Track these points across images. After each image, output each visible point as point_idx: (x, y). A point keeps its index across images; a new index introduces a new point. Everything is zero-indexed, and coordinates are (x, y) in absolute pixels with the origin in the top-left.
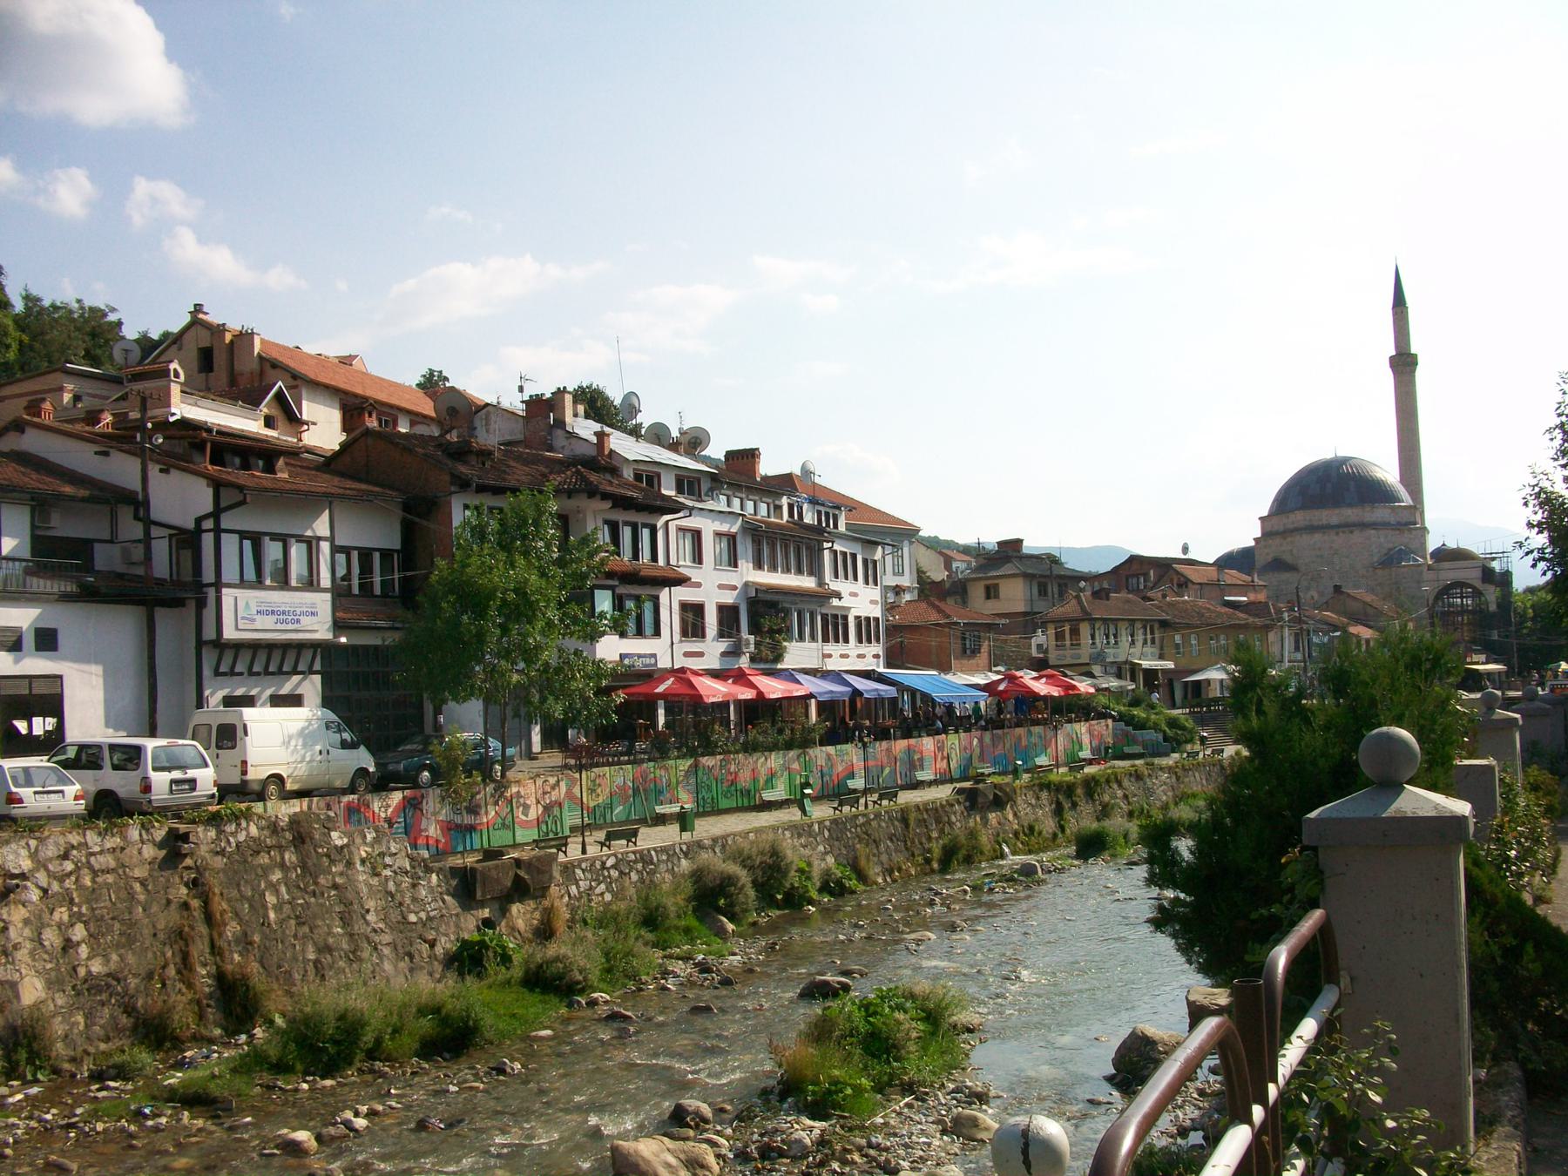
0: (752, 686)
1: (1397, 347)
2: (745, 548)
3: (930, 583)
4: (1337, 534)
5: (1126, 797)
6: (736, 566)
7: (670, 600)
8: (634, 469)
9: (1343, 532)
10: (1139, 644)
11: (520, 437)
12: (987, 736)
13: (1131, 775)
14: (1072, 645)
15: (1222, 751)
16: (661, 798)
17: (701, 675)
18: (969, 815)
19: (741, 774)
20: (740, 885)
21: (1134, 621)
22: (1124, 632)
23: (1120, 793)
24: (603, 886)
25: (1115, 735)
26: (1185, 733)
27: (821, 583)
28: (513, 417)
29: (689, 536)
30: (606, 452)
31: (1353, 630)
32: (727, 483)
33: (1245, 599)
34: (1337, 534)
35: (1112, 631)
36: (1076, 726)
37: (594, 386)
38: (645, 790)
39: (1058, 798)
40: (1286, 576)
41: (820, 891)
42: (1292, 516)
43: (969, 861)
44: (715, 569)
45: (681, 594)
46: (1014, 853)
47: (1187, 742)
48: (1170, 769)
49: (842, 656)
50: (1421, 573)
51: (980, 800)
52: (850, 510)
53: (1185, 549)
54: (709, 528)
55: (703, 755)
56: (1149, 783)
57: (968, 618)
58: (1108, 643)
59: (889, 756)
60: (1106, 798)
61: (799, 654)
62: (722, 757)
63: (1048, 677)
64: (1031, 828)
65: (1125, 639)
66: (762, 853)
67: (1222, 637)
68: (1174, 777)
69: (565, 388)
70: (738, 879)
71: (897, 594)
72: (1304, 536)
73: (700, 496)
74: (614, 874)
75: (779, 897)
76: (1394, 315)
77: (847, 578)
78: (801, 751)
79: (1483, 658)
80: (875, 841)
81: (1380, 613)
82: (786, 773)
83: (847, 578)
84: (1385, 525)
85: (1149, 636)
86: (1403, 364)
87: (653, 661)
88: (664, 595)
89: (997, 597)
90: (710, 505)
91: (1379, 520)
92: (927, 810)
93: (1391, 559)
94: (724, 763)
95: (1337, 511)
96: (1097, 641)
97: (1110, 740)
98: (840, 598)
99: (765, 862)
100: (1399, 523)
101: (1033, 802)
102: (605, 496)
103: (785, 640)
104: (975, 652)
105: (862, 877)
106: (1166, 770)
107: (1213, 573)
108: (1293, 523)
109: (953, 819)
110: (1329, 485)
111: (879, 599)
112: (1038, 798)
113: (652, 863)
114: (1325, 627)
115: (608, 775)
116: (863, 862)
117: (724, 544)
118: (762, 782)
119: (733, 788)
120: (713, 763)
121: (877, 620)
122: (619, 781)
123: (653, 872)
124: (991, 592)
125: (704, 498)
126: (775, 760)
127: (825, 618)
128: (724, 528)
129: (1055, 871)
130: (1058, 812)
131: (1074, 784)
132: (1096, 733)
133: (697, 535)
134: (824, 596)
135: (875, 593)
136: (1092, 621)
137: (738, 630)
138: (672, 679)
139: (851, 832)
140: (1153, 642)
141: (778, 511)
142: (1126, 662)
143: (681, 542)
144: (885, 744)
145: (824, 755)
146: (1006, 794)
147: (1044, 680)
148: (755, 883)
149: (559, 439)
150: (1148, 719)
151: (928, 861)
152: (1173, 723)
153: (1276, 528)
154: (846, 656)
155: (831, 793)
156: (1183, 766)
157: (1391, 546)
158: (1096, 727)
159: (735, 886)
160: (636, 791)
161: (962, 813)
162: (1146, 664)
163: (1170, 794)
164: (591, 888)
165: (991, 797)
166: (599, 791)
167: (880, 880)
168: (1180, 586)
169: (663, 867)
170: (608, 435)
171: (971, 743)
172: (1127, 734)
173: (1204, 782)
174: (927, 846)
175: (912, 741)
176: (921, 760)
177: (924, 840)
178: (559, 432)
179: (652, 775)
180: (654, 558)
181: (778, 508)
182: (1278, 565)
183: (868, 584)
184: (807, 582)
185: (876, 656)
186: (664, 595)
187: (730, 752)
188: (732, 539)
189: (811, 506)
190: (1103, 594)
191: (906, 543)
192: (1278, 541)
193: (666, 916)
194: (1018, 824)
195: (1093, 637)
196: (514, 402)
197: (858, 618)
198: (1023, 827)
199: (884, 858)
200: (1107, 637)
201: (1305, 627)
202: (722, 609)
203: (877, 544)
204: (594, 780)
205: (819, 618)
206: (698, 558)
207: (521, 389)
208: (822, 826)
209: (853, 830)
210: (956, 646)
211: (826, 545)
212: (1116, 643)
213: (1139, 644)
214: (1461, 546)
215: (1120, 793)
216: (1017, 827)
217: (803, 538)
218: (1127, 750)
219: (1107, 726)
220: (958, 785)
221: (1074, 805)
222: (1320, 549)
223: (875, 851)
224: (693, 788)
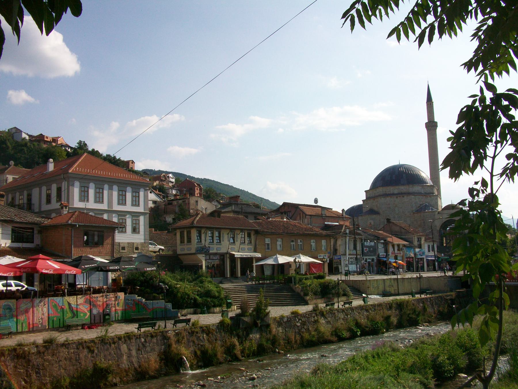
4: (397, 197)
9: (399, 197)
22: (226, 236)
31: (389, 239)
34: (397, 197)
35: (216, 234)
40: (374, 216)
47: (215, 306)
50: (434, 215)
53: (316, 201)
67: (299, 241)
72: (382, 199)
81: (407, 232)
84: (420, 194)
91: (416, 191)
93: (421, 209)
95: (397, 187)
100: (426, 193)
114: (372, 237)
140: (250, 242)
142: (227, 253)
153: (371, 196)
157: (421, 203)
172: (138, 303)
173: (134, 353)
182: (372, 212)
190: (216, 214)
213: (238, 243)
222: (389, 204)
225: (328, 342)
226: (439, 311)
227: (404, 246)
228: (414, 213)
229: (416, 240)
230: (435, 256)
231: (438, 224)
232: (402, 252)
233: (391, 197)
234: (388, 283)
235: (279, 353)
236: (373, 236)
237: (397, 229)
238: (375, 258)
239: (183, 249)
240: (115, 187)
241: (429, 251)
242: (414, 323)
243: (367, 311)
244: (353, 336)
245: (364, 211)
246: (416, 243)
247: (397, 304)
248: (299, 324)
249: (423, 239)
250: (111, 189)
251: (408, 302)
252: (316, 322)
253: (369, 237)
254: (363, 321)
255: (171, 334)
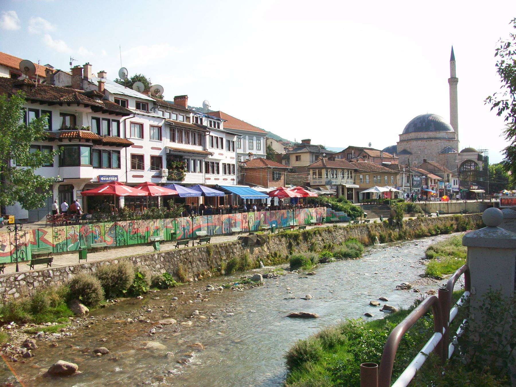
0: (148, 190)
1: (451, 75)
2: (166, 133)
3: (276, 155)
5: (323, 240)
6: (161, 140)
7: (126, 154)
8: (115, 98)
10: (346, 178)
11: (70, 84)
12: (268, 213)
13: (326, 231)
14: (319, 178)
15: (369, 221)
16: (96, 240)
17: (122, 185)
18: (244, 249)
19: (140, 229)
20: (93, 288)
21: (344, 169)
22: (340, 173)
23: (320, 238)
24: (14, 290)
25: (327, 213)
26: (358, 213)
27: (205, 149)
28: (67, 75)
29: (138, 126)
30: (102, 90)
31: (429, 176)
32: (160, 105)
33: (390, 163)
34: (426, 141)
35: (335, 172)
36: (310, 209)
37: (141, 76)
38: (86, 236)
39: (290, 241)
40: (407, 156)
41: (152, 287)
42: (410, 135)
43: (242, 269)
44: (150, 141)
45: (131, 150)
46: (265, 266)
48: (344, 228)
49: (215, 179)
50: (456, 156)
51: (250, 242)
52: (225, 121)
53: (370, 145)
54: (147, 123)
55: (120, 221)
56: (334, 234)
57: (275, 166)
58: (333, 177)
59: (219, 221)
60: (313, 240)
61: (190, 178)
62: (130, 221)
63: (298, 189)
64: (276, 254)
65: (340, 176)
66: (113, 271)
68: (346, 232)
69: (89, 63)
70: (92, 285)
71: (249, 156)
73: (148, 110)
74: (23, 283)
75: (124, 292)
76: (451, 63)
77: (218, 147)
78: (173, 219)
79: (477, 187)
80: (190, 262)
81: (440, 170)
82: (165, 229)
83: (218, 147)
84: (444, 139)
85: (350, 175)
86: (453, 81)
87: (116, 179)
88: (123, 151)
89: (300, 159)
90: (152, 114)
91: (442, 137)
92: (221, 247)
93: (445, 151)
94: (131, 224)
95: (427, 133)
96: (329, 176)
97: (325, 215)
98: (212, 155)
99: (114, 276)
100: (449, 138)
101: (278, 242)
102: (86, 106)
103: (185, 172)
104: (279, 179)
105: (180, 279)
106: (343, 229)
107: (378, 154)
108: (411, 137)
109: (235, 250)
110: (424, 124)
111: (235, 157)
112: (280, 241)
113: (49, 276)
115: (65, 230)
116: (182, 272)
117: (156, 130)
118: (151, 232)
119: (135, 235)
120: (125, 224)
121: (234, 165)
122: (72, 232)
123: (48, 282)
124: (298, 158)
125: (149, 111)
126: (159, 223)
127: (207, 164)
128: (156, 123)
129: (273, 277)
130: (290, 246)
131: (298, 235)
132: (319, 212)
133: (141, 126)
134: (206, 154)
135: (233, 154)
136: (327, 169)
137: (162, 167)
138: (108, 187)
139: (177, 258)
140: (351, 177)
141: (187, 119)
142: (340, 185)
143: (133, 129)
144: (217, 216)
145: (185, 221)
146: (263, 239)
147: (296, 191)
148: (106, 287)
149: (86, 85)
150: (342, 207)
151: (219, 270)
152: (353, 209)
154: (218, 179)
155: (188, 237)
156: (350, 227)
157: (445, 146)
158: (319, 210)
159: (90, 289)
160: (81, 237)
161: (240, 248)
162: (348, 186)
163: (343, 239)
164: (5, 291)
165: (255, 241)
166: (60, 237)
167: (191, 280)
168: (364, 157)
169: (57, 278)
170: (103, 83)
171: (260, 216)
172: (332, 213)
173: (359, 233)
174: (219, 263)
175: (231, 215)
176: (235, 223)
177: (218, 260)
178: (86, 82)
179: (91, 230)
180: (119, 135)
181: (188, 118)
182: (405, 152)
183: (229, 150)
184: (198, 148)
185: (233, 180)
186: (123, 151)
187: (135, 220)
188: (160, 128)
189: (207, 119)
190: (332, 159)
191: (262, 138)
192: (405, 143)
193: (43, 307)
194: (269, 252)
195: (327, 175)
196: (67, 69)
197: (224, 165)
198: (271, 253)
199: (195, 269)
200: (333, 175)
201: (411, 174)
202: (153, 158)
203: (235, 135)
204: (57, 232)
205: (204, 163)
206: (142, 135)
207: (71, 64)
208: (160, 256)
209: (178, 257)
210: (270, 176)
211: (207, 133)
212: (337, 177)
213: (346, 178)
214: (470, 147)
215: (320, 238)
216: (268, 253)
217: (195, 130)
218: (332, 219)
219: (324, 209)
220: (240, 235)
221: (298, 244)
223: (190, 266)
224: (114, 235)
225: (427, 236)
226: (477, 224)
227: (438, 180)
228: (440, 154)
229: (446, 176)
230: (459, 189)
231: (458, 162)
232: (436, 185)
233: (421, 141)
234: (442, 206)
235: (407, 239)
236: (419, 173)
237: (430, 167)
238: (420, 189)
239: (314, 182)
240: (247, 137)
241: (454, 185)
242: (464, 229)
243: (441, 220)
244: (436, 235)
245: (398, 152)
246: (446, 179)
247: (455, 218)
248: (413, 225)
249: (451, 175)
250: (245, 138)
251: (460, 216)
252: (420, 224)
253: (417, 174)
254: (441, 227)
255: (369, 226)
